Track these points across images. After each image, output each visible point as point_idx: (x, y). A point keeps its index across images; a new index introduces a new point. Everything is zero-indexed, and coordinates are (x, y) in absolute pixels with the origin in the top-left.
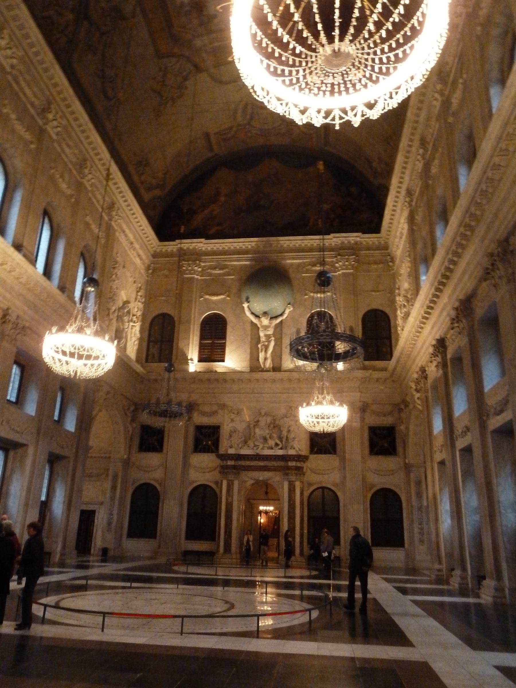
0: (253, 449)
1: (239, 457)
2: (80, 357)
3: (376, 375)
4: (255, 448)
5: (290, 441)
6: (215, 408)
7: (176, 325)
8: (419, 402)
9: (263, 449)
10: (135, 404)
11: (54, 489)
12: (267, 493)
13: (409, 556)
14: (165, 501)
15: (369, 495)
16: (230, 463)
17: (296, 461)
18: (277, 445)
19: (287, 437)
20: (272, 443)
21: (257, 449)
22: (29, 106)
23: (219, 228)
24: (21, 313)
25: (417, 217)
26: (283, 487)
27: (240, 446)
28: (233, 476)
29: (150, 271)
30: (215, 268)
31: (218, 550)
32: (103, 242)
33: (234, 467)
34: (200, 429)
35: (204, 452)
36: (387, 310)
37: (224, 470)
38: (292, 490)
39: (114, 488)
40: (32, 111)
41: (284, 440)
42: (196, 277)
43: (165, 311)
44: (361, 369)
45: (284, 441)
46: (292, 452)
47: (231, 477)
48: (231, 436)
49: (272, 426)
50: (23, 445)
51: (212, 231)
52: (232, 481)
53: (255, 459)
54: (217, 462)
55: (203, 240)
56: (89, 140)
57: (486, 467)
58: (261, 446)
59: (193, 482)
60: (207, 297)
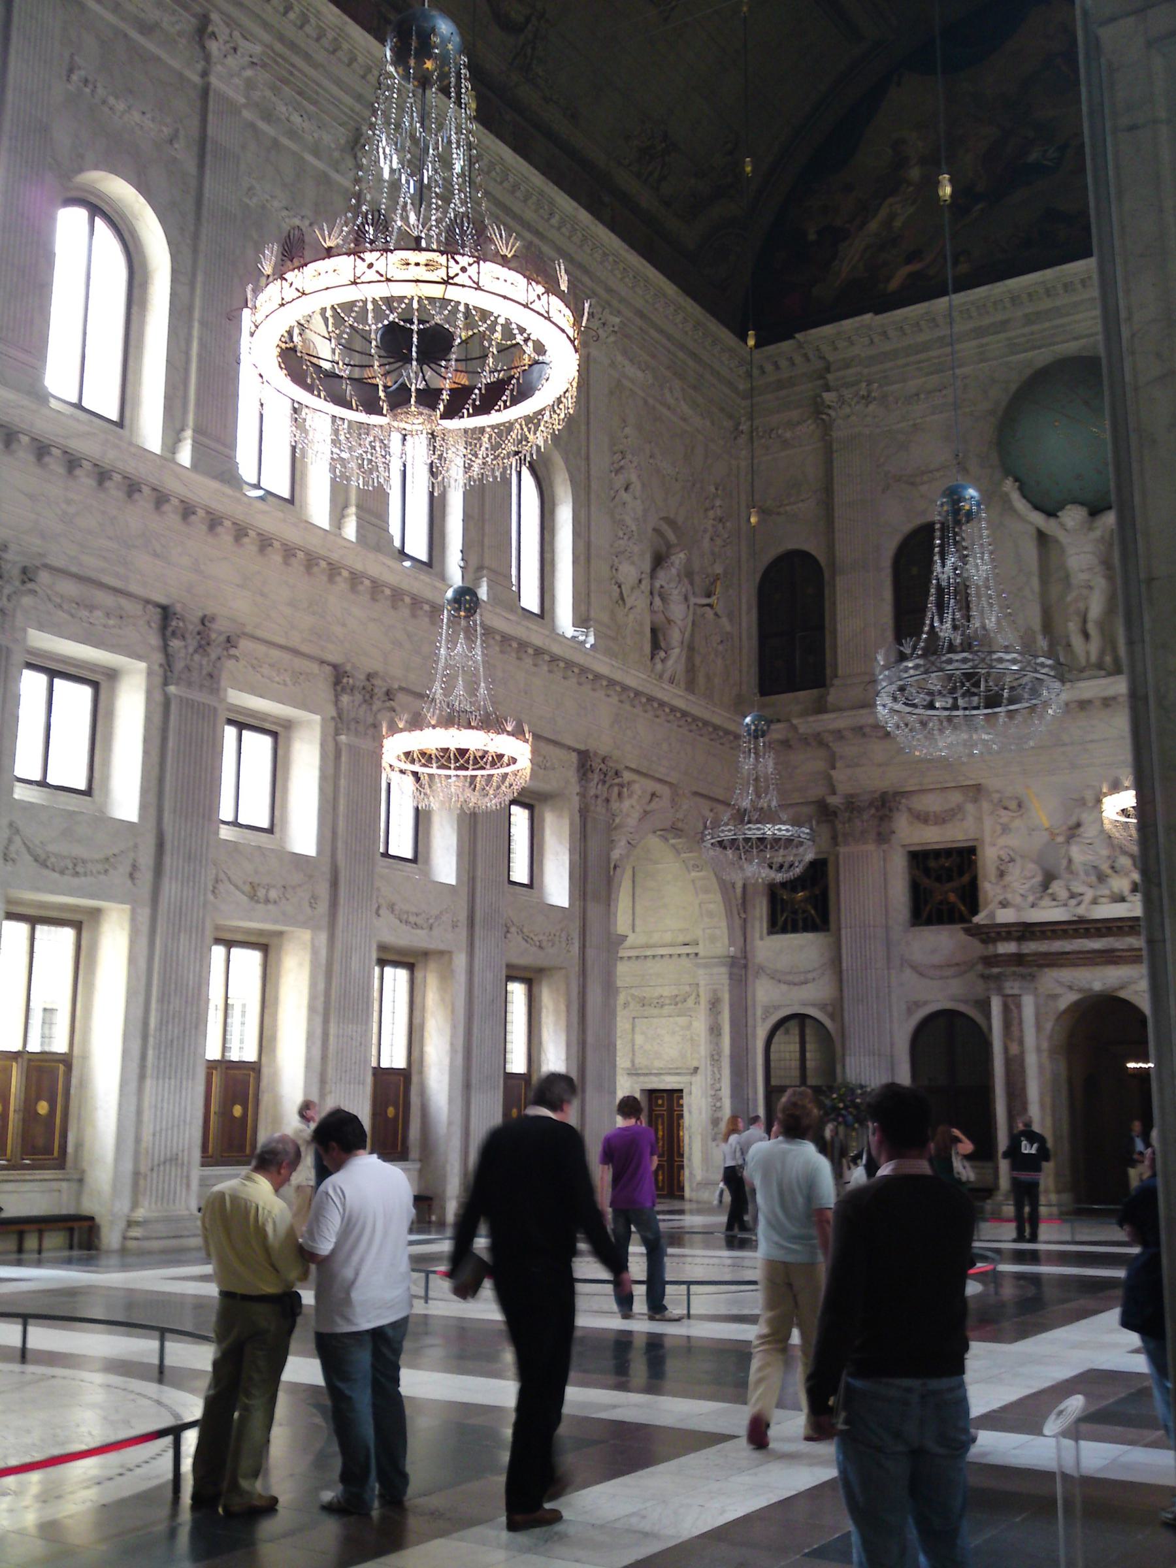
0: (1065, 905)
1: (1027, 931)
4: (1073, 902)
7: (827, 575)
9: (1095, 902)
11: (540, 1043)
14: (848, 1059)
16: (1007, 948)
21: (1079, 904)
22: (309, 158)
27: (1031, 899)
28: (1017, 984)
29: (743, 440)
33: (1019, 959)
34: (919, 859)
37: (993, 970)
40: (320, 165)
43: (791, 545)
50: (441, 953)
51: (894, 285)
52: (1017, 997)
54: (976, 948)
55: (868, 317)
58: (1089, 894)
59: (917, 1005)
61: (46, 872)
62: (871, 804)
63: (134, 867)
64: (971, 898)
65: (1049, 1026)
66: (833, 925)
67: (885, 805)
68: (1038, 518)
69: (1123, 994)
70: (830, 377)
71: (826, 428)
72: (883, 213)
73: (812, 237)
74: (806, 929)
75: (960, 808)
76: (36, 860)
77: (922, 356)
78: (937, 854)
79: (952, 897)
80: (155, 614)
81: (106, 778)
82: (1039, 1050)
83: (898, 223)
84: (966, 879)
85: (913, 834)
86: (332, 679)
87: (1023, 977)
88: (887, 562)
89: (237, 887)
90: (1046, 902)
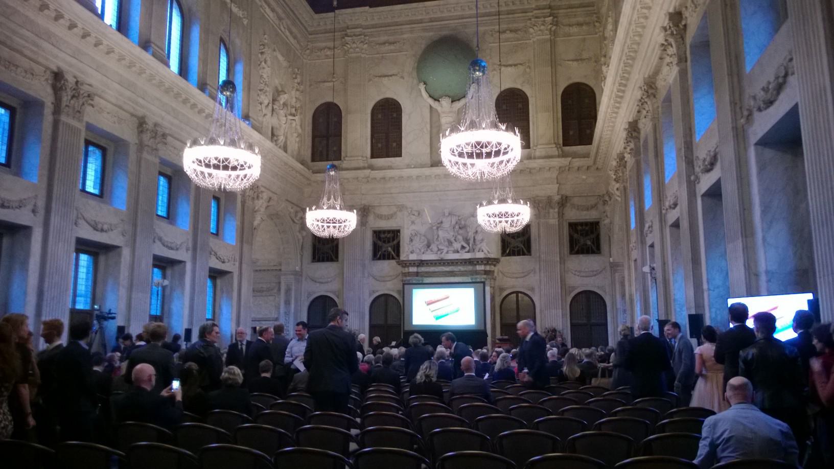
1: (421, 263)
2: (226, 168)
3: (577, 162)
5: (477, 243)
6: (395, 209)
8: (618, 193)
9: (447, 252)
15: (569, 299)
16: (413, 269)
17: (485, 265)
18: (463, 247)
19: (474, 239)
20: (457, 246)
24: (159, 120)
29: (308, 51)
30: (384, 43)
32: (245, 23)
33: (417, 274)
35: (384, 259)
36: (591, 83)
39: (287, 303)
41: (471, 242)
42: (363, 56)
44: (559, 156)
45: (470, 242)
46: (480, 255)
48: (412, 240)
49: (457, 227)
50: (180, 262)
54: (400, 269)
55: (367, 8)
59: (374, 292)
60: (376, 79)
63: (35, 206)
64: (397, 249)
68: (431, 101)
70: (348, 31)
75: (395, 213)
78: (384, 232)
84: (395, 242)
86: (136, 125)
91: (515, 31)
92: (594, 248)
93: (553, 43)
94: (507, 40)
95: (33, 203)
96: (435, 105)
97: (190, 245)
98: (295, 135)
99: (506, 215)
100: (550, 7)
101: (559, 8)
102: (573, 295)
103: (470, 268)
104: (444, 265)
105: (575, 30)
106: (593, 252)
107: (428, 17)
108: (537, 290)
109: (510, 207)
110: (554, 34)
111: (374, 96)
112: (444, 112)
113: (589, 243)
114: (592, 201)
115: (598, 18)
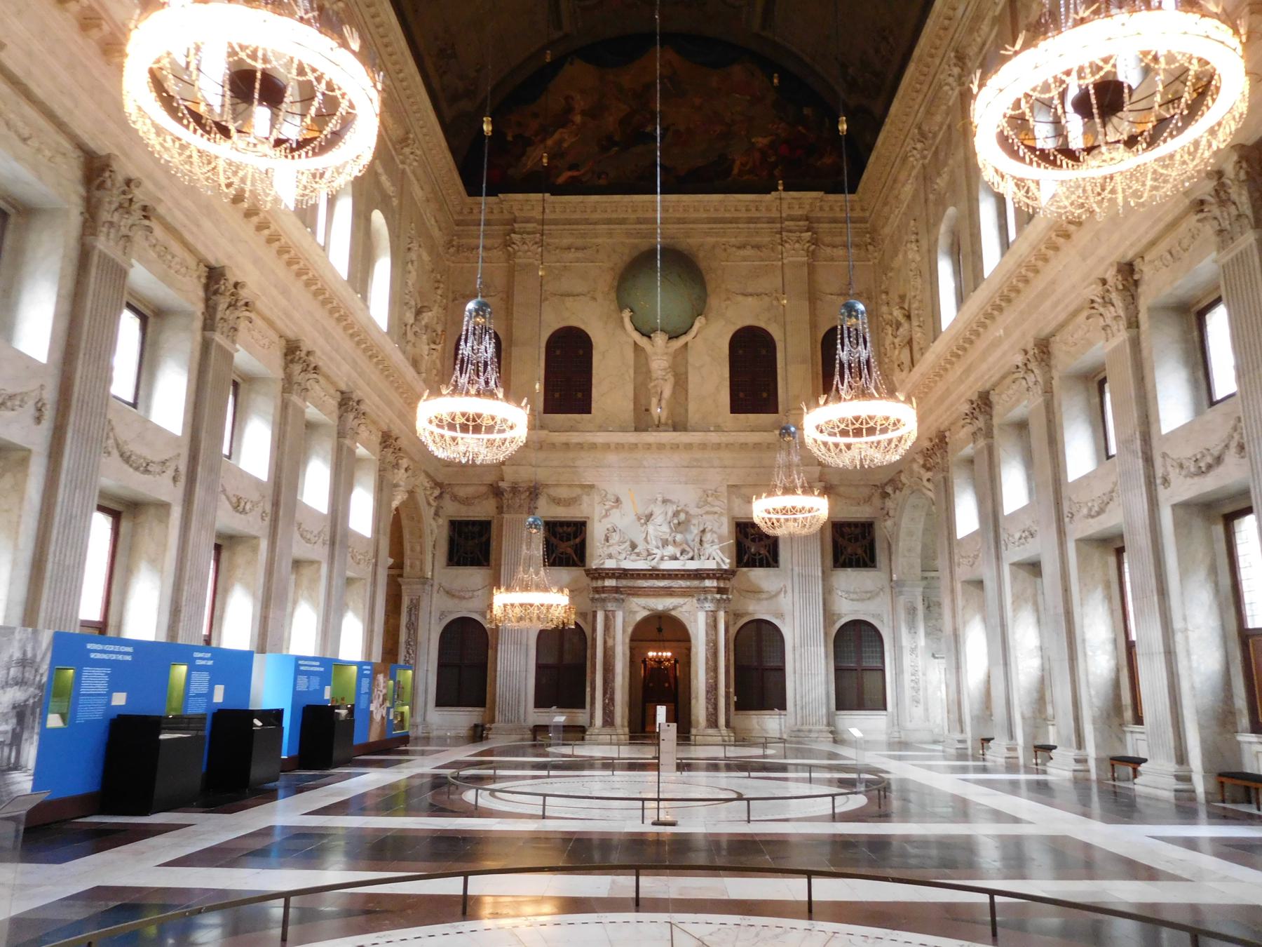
8: (930, 486)
10: (438, 484)
12: (660, 630)
13: (897, 723)
17: (718, 579)
23: (575, 174)
25: (938, 181)
26: (696, 621)
29: (452, 250)
30: (569, 248)
31: (591, 724)
33: (617, 590)
38: (713, 625)
46: (711, 565)
47: (610, 606)
50: (312, 562)
51: (561, 180)
53: (651, 577)
54: (587, 580)
56: (377, 20)
57: (1066, 590)
61: (126, 467)
62: (528, 489)
63: (176, 470)
65: (630, 630)
66: (493, 562)
67: (534, 492)
68: (636, 336)
69: (673, 613)
70: (516, 225)
71: (510, 256)
72: (557, 136)
73: (510, 138)
74: (472, 564)
76: (122, 455)
77: (575, 227)
78: (562, 524)
79: (569, 551)
80: (203, 271)
81: (149, 396)
82: (623, 643)
83: (565, 145)
84: (578, 540)
85: (548, 510)
87: (617, 600)
88: (543, 345)
89: (228, 498)
90: (633, 557)
91: (758, 247)
92: (867, 560)
93: (812, 270)
94: (745, 259)
95: (173, 467)
96: (643, 342)
97: (328, 538)
98: (435, 372)
99: (794, 510)
100: (807, 219)
101: (819, 220)
102: (838, 626)
103: (696, 583)
104: (657, 577)
105: (840, 252)
106: (865, 565)
107: (633, 216)
108: (788, 619)
109: (799, 500)
110: (812, 255)
111: (552, 322)
112: (655, 354)
113: (859, 551)
114: (867, 491)
115: (873, 239)
